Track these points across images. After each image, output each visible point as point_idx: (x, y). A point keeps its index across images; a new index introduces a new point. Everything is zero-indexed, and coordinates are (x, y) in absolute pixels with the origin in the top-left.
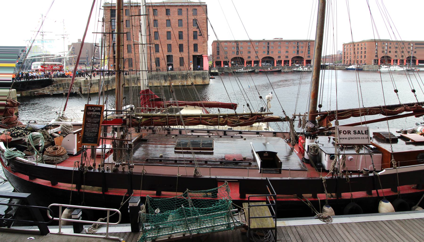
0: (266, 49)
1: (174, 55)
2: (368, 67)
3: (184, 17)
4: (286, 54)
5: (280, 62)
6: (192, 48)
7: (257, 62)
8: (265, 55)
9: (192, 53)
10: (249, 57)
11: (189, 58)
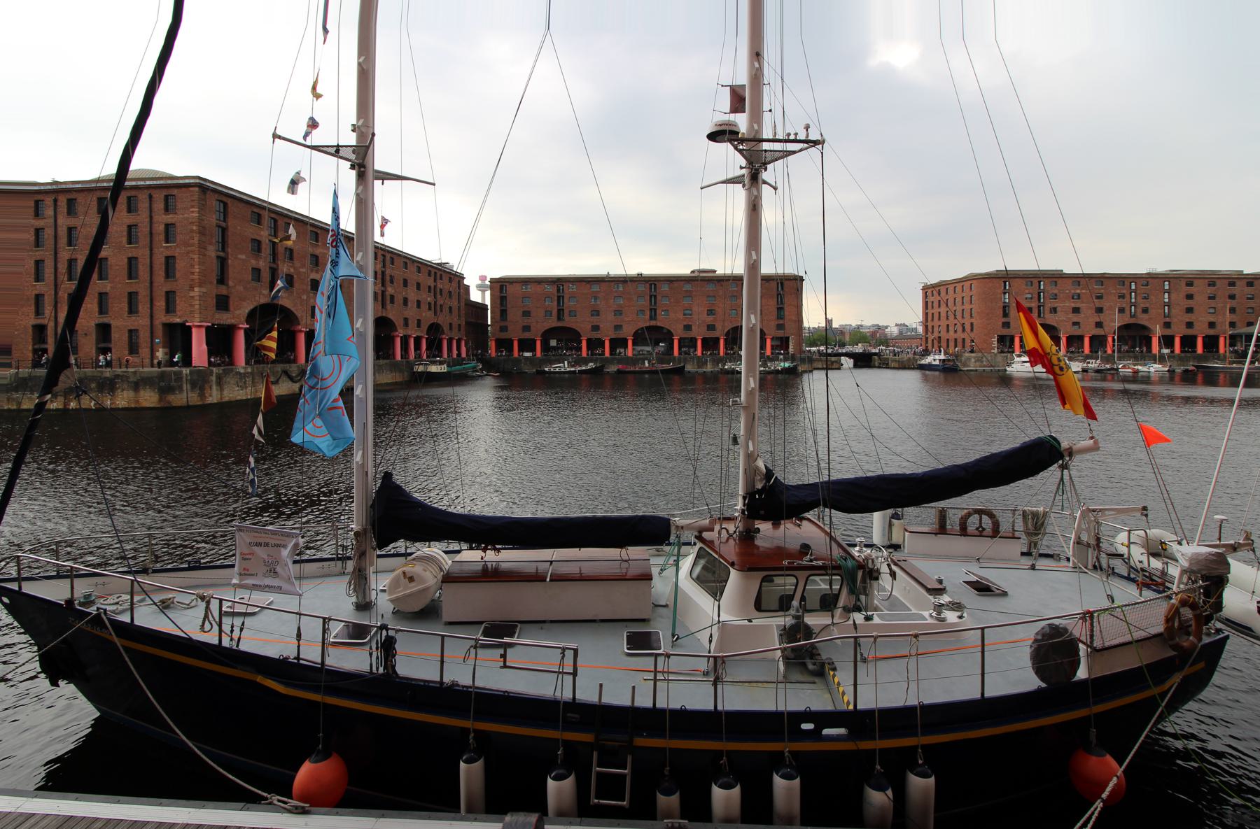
0: (644, 302)
1: (113, 323)
2: (979, 360)
3: (141, 218)
4: (710, 319)
5: (688, 343)
6: (160, 304)
7: (618, 343)
8: (644, 321)
9: (162, 318)
10: (596, 328)
11: (152, 333)
